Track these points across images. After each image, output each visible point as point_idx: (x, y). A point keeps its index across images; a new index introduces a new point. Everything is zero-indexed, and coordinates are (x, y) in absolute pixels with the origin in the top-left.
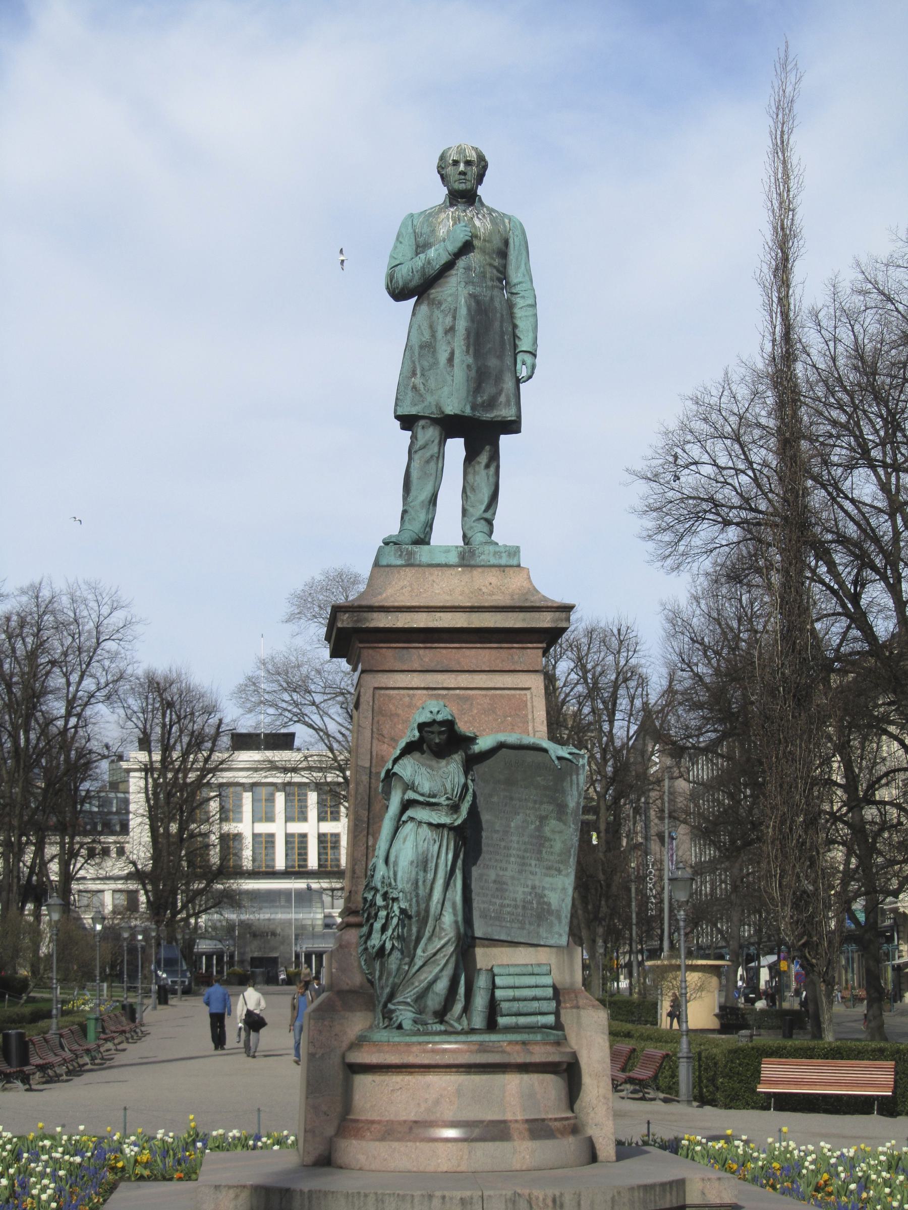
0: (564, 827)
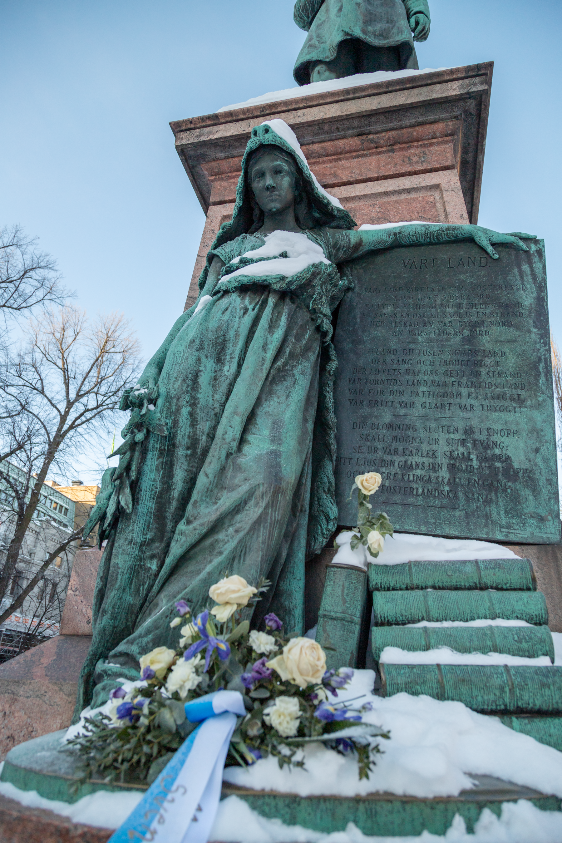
0: (517, 333)
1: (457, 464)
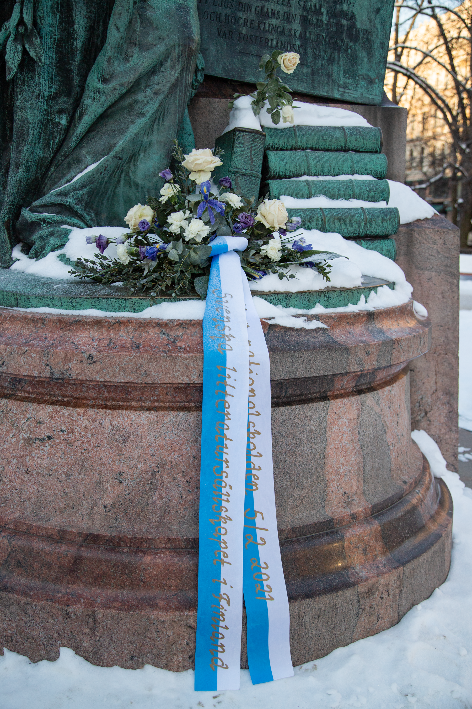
1: (309, 17)
